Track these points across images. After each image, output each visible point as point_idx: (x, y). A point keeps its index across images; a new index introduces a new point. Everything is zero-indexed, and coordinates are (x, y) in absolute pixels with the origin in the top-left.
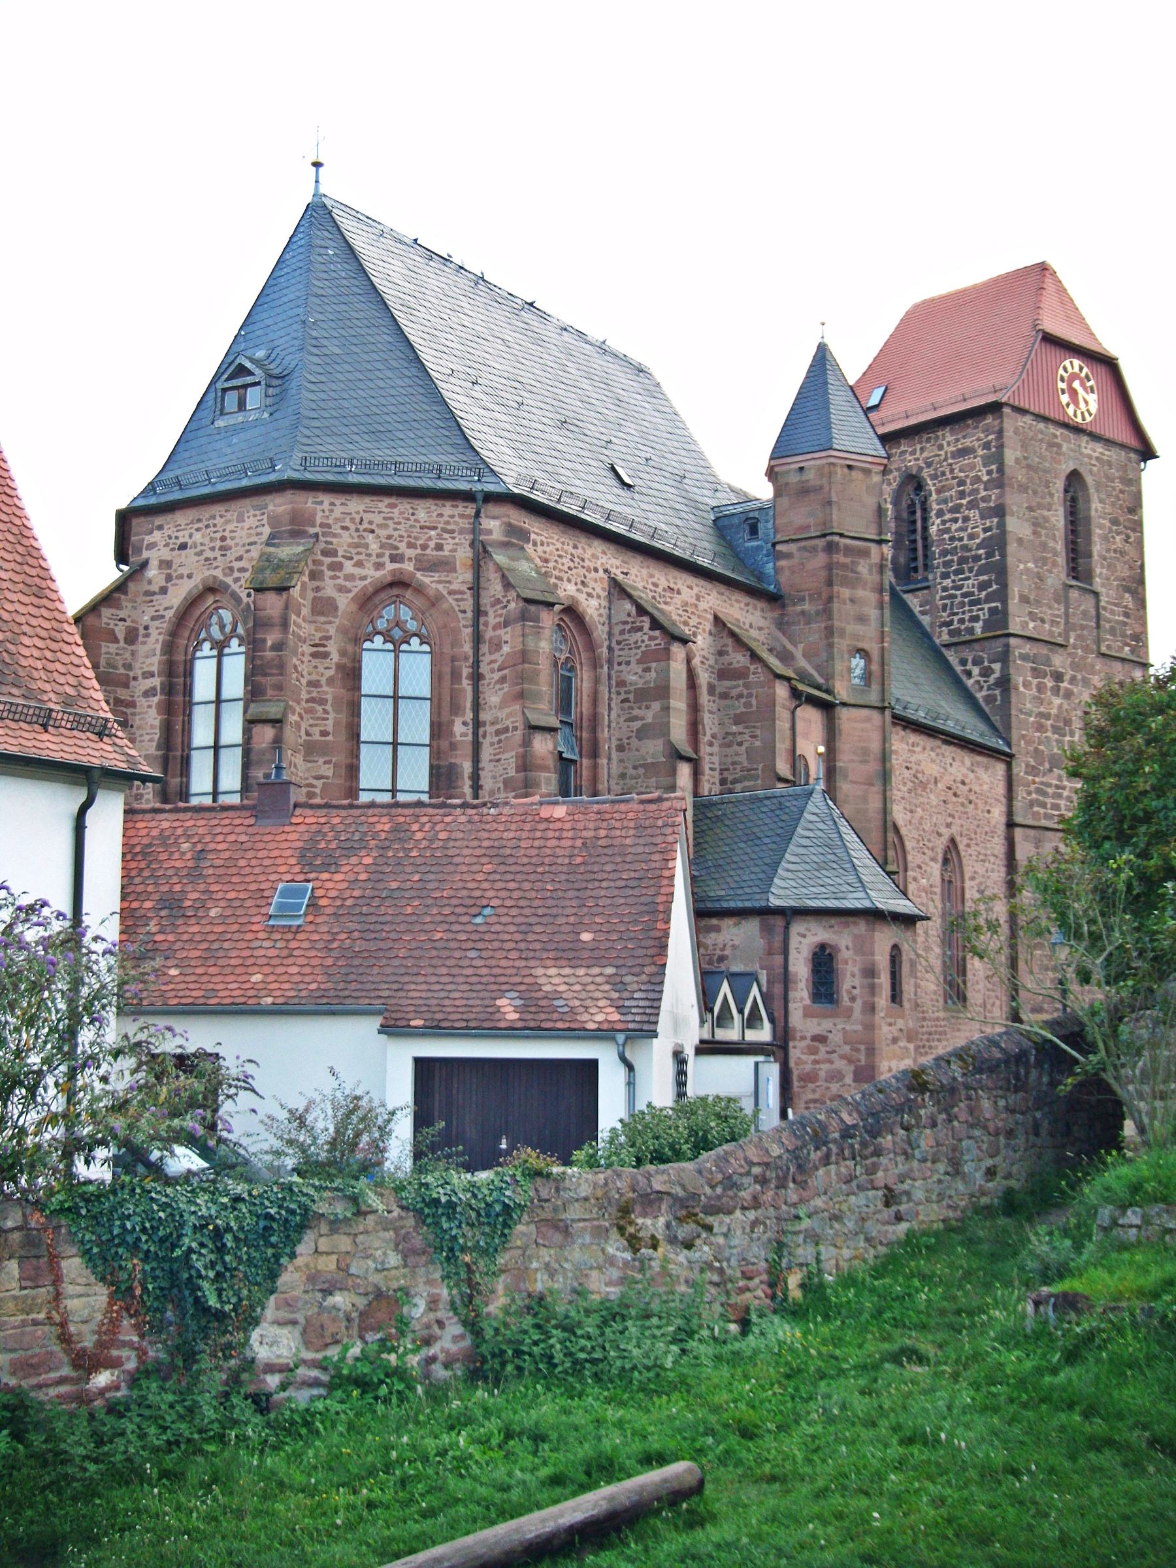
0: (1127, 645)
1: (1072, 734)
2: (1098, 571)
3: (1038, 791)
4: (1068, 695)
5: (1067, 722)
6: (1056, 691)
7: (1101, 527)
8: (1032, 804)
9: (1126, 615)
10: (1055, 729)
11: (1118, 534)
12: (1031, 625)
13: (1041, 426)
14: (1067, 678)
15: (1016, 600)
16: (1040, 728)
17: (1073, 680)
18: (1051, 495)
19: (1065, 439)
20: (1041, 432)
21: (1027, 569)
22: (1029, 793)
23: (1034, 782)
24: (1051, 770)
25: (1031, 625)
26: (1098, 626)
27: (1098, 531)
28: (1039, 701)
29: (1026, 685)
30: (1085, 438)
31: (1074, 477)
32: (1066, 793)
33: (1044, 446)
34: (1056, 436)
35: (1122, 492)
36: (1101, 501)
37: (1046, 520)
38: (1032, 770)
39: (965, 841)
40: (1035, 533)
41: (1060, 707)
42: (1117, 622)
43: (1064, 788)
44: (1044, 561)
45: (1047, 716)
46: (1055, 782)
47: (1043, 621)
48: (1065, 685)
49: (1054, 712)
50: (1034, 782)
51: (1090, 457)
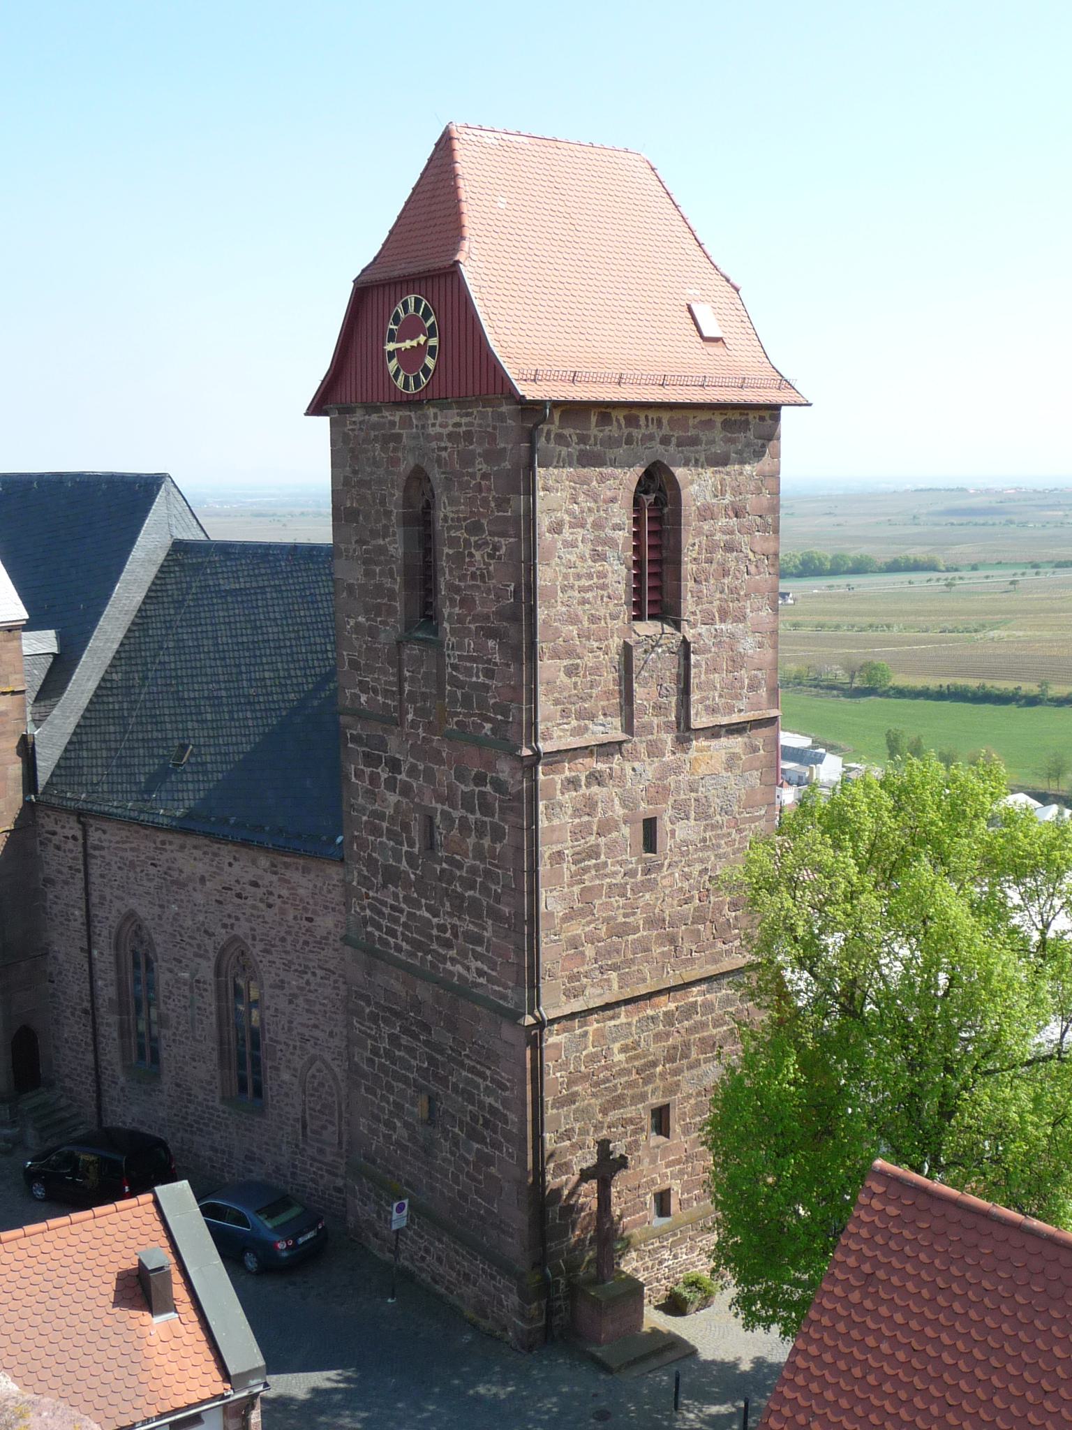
0: (488, 720)
1: (411, 845)
2: (446, 612)
3: (373, 908)
4: (406, 791)
5: (406, 827)
6: (391, 784)
7: (453, 542)
8: (365, 921)
9: (489, 674)
10: (391, 834)
11: (478, 546)
14: (404, 768)
16: (376, 831)
17: (413, 771)
18: (388, 514)
19: (406, 423)
20: (375, 426)
21: (358, 624)
22: (363, 908)
23: (368, 897)
24: (384, 886)
25: (363, 698)
26: (441, 694)
27: (446, 550)
28: (371, 795)
29: (359, 774)
30: (432, 411)
31: (419, 477)
32: (403, 919)
34: (393, 424)
35: (485, 476)
37: (382, 550)
38: (364, 881)
39: (260, 946)
40: (368, 574)
41: (398, 804)
42: (476, 686)
43: (401, 911)
44: (378, 610)
45: (381, 816)
46: (391, 901)
47: (375, 691)
48: (403, 777)
49: (390, 811)
50: (368, 897)
51: (439, 437)
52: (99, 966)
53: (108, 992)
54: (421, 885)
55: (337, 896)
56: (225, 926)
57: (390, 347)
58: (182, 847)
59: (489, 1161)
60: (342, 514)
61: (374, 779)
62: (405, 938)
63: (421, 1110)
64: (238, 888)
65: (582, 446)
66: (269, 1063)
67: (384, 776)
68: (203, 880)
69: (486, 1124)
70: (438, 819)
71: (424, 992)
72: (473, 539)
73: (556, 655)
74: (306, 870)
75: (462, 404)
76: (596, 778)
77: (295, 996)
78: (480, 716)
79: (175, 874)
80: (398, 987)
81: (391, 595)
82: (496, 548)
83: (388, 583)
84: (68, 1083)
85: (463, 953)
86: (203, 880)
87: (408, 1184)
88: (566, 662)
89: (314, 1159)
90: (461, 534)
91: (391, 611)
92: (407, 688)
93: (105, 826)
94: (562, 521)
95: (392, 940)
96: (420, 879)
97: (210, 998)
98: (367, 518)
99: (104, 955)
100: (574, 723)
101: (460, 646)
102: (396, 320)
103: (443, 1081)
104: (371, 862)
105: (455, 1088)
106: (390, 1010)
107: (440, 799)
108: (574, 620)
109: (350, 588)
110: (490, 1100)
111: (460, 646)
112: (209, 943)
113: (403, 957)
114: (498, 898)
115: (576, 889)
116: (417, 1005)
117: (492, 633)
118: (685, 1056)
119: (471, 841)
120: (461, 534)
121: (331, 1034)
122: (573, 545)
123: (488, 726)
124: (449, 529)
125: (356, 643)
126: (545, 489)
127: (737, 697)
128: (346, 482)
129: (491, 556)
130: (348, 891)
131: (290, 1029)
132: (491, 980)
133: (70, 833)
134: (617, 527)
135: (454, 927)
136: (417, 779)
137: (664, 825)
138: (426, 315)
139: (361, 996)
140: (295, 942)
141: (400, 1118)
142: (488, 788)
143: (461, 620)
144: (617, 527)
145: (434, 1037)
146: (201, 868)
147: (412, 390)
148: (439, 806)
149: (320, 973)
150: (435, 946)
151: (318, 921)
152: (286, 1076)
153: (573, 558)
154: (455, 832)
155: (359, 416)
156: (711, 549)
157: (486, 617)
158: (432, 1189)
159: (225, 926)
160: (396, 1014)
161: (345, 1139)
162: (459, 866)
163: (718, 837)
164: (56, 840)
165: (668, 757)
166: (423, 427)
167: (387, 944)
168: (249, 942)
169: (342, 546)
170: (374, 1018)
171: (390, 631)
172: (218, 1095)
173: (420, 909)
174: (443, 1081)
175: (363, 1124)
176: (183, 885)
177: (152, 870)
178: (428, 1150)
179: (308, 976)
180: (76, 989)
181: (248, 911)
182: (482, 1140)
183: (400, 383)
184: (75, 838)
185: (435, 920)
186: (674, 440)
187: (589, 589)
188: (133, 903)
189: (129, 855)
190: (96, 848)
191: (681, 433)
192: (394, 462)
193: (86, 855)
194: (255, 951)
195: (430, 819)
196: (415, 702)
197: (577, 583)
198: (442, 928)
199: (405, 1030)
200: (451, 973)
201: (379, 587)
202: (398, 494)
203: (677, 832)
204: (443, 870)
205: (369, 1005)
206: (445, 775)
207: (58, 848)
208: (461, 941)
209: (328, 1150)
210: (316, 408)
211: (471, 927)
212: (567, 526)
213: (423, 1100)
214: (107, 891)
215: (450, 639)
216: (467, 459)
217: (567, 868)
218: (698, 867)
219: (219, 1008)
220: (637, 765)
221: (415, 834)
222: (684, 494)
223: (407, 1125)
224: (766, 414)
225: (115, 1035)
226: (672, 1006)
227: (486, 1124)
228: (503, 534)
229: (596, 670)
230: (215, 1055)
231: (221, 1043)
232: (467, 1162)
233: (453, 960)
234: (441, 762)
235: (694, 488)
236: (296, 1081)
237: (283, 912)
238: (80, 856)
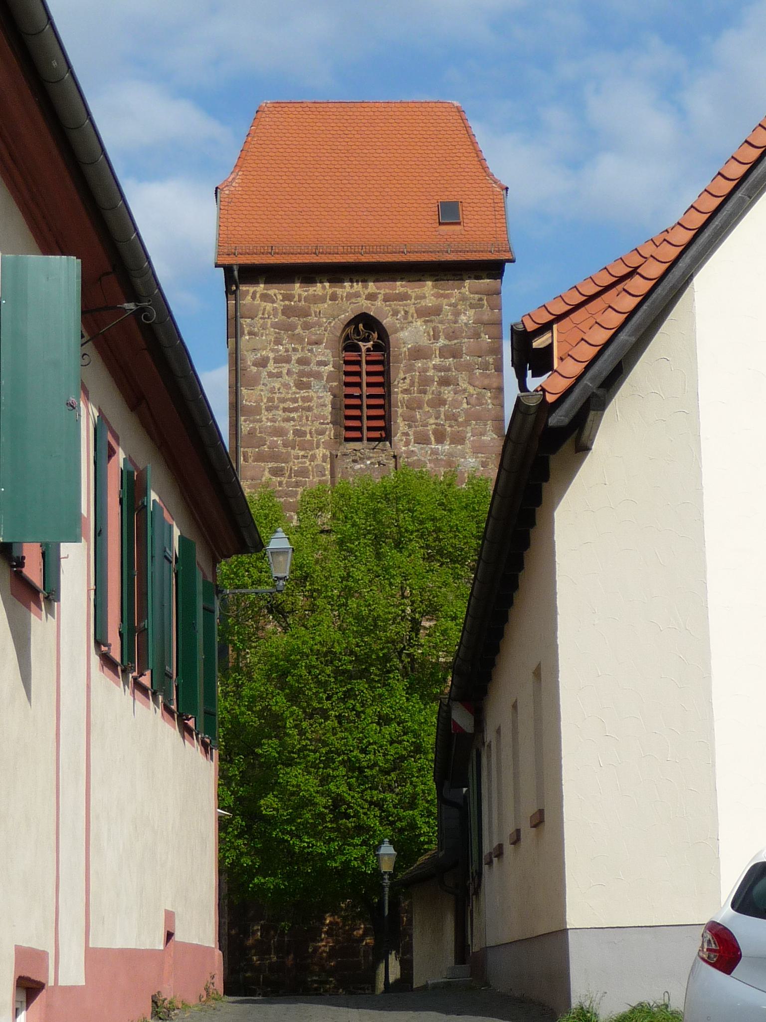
65: (287, 303)
73: (260, 458)
94: (268, 358)
108: (280, 432)
122: (279, 375)
126: (250, 333)
153: (277, 385)
186: (380, 297)
187: (295, 410)
191: (387, 291)
197: (282, 406)
212: (271, 362)
229: (303, 472)
235: (404, 335)
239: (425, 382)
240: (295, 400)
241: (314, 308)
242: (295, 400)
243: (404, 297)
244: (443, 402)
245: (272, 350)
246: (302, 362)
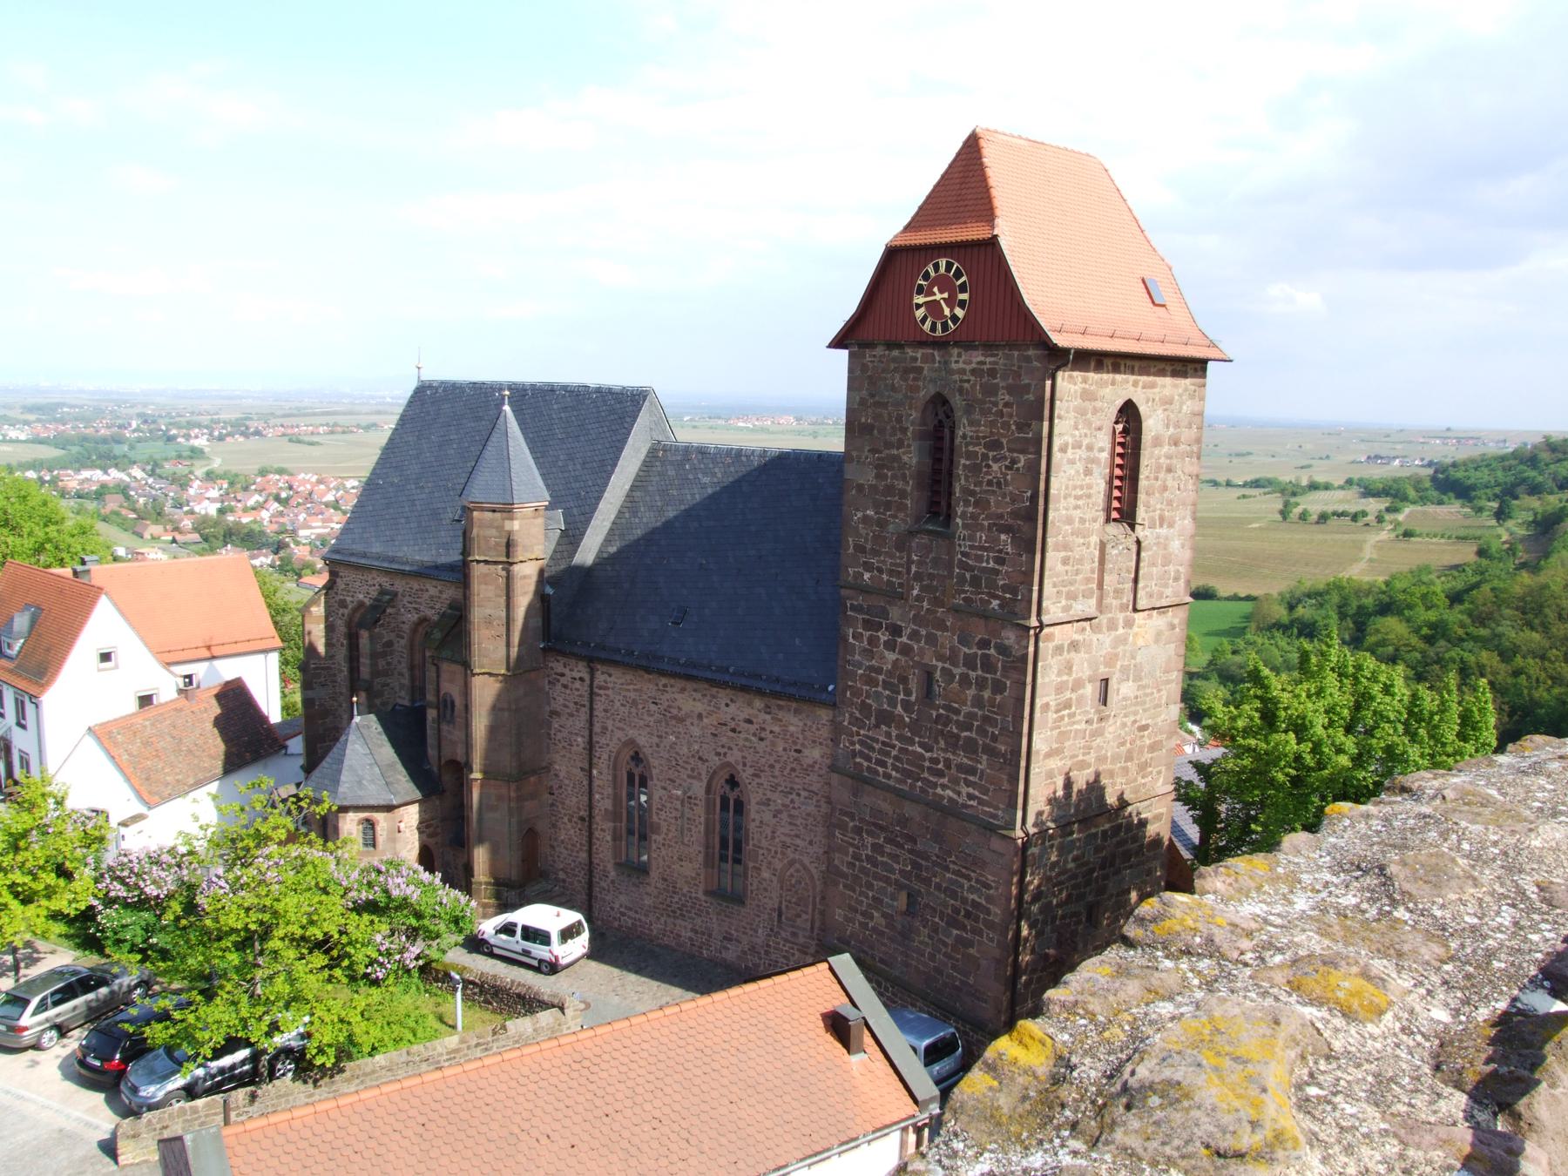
0: (996, 597)
2: (959, 510)
3: (861, 743)
4: (906, 650)
6: (890, 646)
7: (969, 455)
8: (854, 754)
10: (886, 685)
11: (996, 460)
12: (867, 576)
13: (896, 353)
15: (851, 550)
16: (871, 682)
17: (914, 635)
18: (904, 430)
19: (928, 359)
20: (894, 360)
21: (865, 517)
22: (853, 743)
24: (877, 726)
25: (867, 576)
27: (963, 461)
28: (869, 653)
29: (857, 636)
30: (955, 351)
32: (894, 753)
33: (897, 376)
34: (916, 359)
35: (1007, 405)
36: (971, 423)
37: (897, 458)
39: (750, 771)
40: (879, 476)
43: (893, 747)
44: (888, 505)
45: (879, 671)
47: (880, 571)
51: (963, 371)
52: (596, 783)
53: (603, 803)
54: (915, 727)
55: (825, 733)
56: (718, 754)
57: (920, 299)
58: (683, 690)
59: (970, 944)
60: (854, 427)
61: (873, 641)
62: (895, 768)
63: (902, 902)
64: (733, 725)
66: (751, 865)
67: (883, 638)
68: (700, 716)
69: (968, 915)
70: (938, 675)
71: (911, 810)
72: (991, 454)
73: (1057, 549)
74: (797, 712)
75: (989, 347)
76: (1074, 646)
77: (779, 812)
78: (989, 594)
79: (675, 711)
80: (886, 807)
81: (903, 494)
82: (1014, 462)
83: (900, 484)
84: (562, 875)
85: (955, 781)
86: (700, 716)
87: (882, 961)
88: (1063, 554)
89: (786, 940)
90: (980, 450)
91: (901, 507)
92: (914, 569)
93: (611, 670)
95: (881, 770)
96: (914, 722)
97: (700, 810)
98: (882, 431)
99: (602, 774)
100: (1064, 602)
101: (972, 538)
102: (926, 276)
103: (927, 882)
104: (865, 708)
105: (938, 887)
106: (875, 825)
107: (941, 658)
108: (1070, 521)
109: (860, 488)
110: (975, 897)
111: (972, 538)
112: (703, 769)
113: (892, 783)
114: (994, 738)
115: (1055, 732)
116: (903, 821)
117: (1007, 529)
118: (1112, 865)
119: (971, 692)
120: (980, 450)
121: (811, 843)
123: (995, 603)
124: (967, 445)
125: (863, 532)
127: (1166, 586)
128: (863, 402)
129: (1009, 468)
130: (837, 729)
131: (773, 838)
132: (981, 802)
133: (577, 675)
134: (1102, 450)
135: (947, 761)
136: (919, 641)
137: (1113, 684)
138: (958, 275)
139: (846, 814)
140: (782, 770)
141: (877, 909)
142: (992, 651)
143: (974, 517)
144: (1102, 450)
145: (919, 847)
146: (700, 707)
147: (939, 333)
148: (940, 665)
149: (803, 793)
150: (926, 775)
151: (806, 752)
152: (766, 875)
154: (955, 685)
155: (879, 351)
156: (1159, 468)
157: (1001, 516)
158: (907, 965)
159: (718, 754)
160: (881, 828)
161: (817, 924)
162: (957, 712)
163: (1146, 695)
164: (563, 680)
165: (1121, 631)
166: (946, 363)
167: (877, 773)
168: (740, 767)
169: (854, 454)
170: (858, 831)
171: (898, 524)
172: (702, 887)
173: (913, 743)
174: (927, 882)
175: (839, 914)
176: (681, 720)
177: (653, 707)
178: (906, 935)
179: (793, 796)
180: (574, 800)
181: (741, 743)
182: (963, 928)
183: (927, 326)
184: (581, 679)
185: (928, 755)
188: (632, 733)
189: (633, 695)
190: (600, 688)
192: (916, 389)
193: (592, 694)
194: (744, 775)
195: (929, 675)
196: (921, 580)
198: (936, 761)
199: (889, 841)
200: (942, 797)
201: (890, 490)
202: (915, 414)
203: (1123, 690)
204: (939, 716)
205: (853, 819)
206: (947, 639)
207: (565, 686)
208: (953, 771)
209: (801, 934)
210: (838, 343)
211: (965, 760)
213: (903, 897)
214: (609, 724)
215: (962, 532)
216: (991, 391)
217: (1052, 716)
218: (1132, 718)
219: (707, 820)
220: (1100, 636)
221: (913, 685)
222: (1144, 425)
223: (884, 915)
224: (1198, 366)
225: (609, 838)
226: (1107, 826)
227: (968, 915)
228: (1023, 452)
229: (1080, 561)
230: (701, 858)
231: (707, 847)
232: (945, 944)
233: (944, 787)
234: (946, 629)
236: (775, 879)
237: (773, 744)
238: (586, 694)
239: (1159, 468)
240: (1082, 488)
241: (1102, 392)
242: (1082, 488)
243: (1153, 386)
244: (1165, 488)
245: (1073, 436)
246: (1090, 448)
